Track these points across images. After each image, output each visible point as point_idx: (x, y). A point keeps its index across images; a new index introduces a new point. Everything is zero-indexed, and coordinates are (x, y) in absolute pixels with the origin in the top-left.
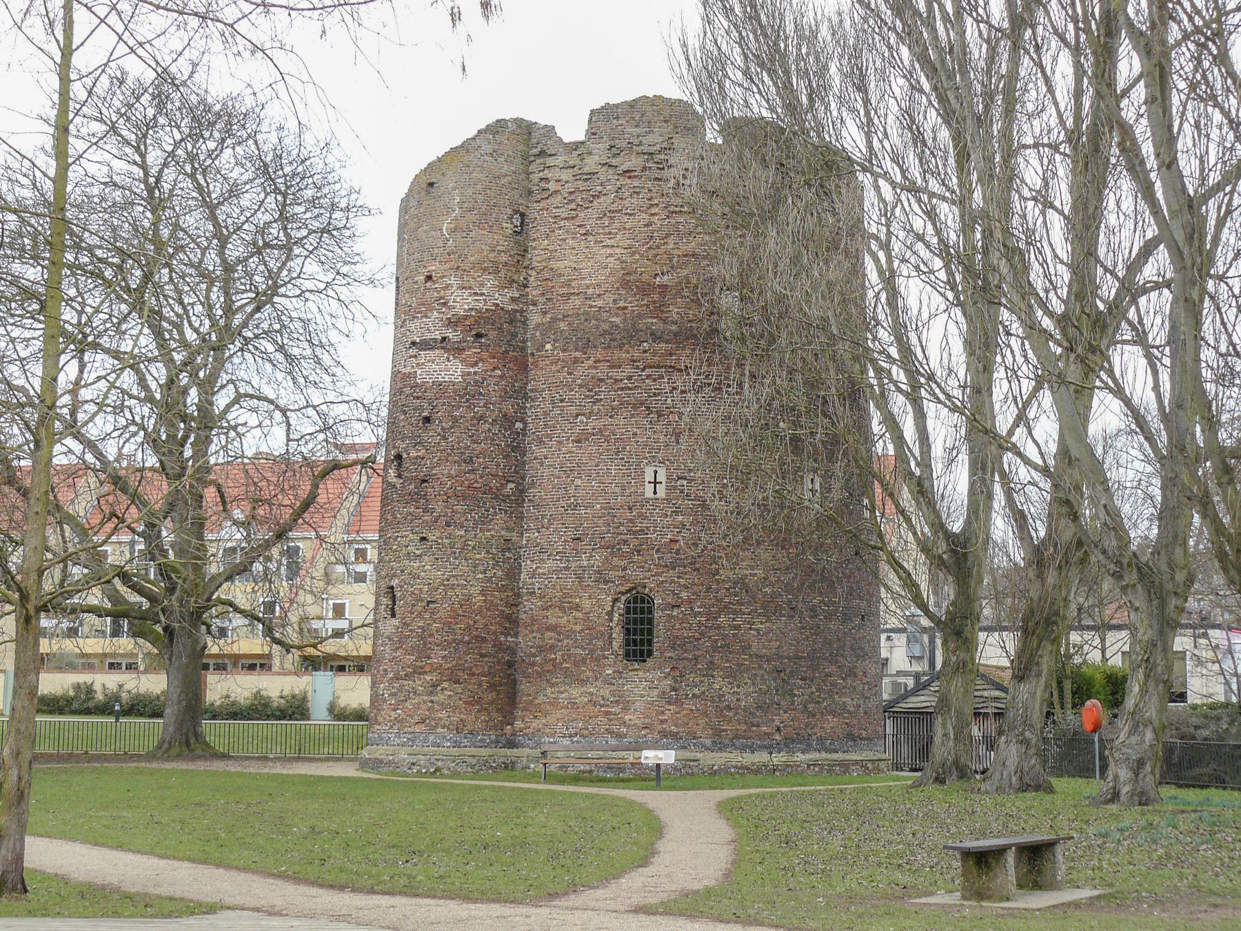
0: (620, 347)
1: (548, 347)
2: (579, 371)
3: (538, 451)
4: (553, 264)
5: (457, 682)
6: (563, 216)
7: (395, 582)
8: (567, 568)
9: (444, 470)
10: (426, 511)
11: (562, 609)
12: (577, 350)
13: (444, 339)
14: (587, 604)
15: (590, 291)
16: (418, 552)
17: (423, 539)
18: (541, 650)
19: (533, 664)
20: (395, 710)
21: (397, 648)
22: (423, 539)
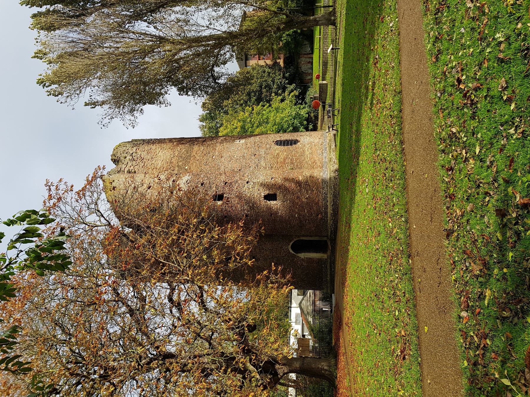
0: (193, 149)
1: (186, 168)
2: (198, 158)
3: (222, 168)
4: (158, 167)
5: (303, 172)
6: (143, 164)
7: (263, 194)
8: (264, 157)
9: (223, 178)
10: (237, 182)
11: (278, 158)
12: (190, 159)
13: (173, 181)
14: (277, 152)
15: (172, 156)
16: (252, 184)
17: (247, 183)
18: (292, 163)
19: (297, 166)
20: (313, 191)
21: (289, 191)
22: (247, 183)
